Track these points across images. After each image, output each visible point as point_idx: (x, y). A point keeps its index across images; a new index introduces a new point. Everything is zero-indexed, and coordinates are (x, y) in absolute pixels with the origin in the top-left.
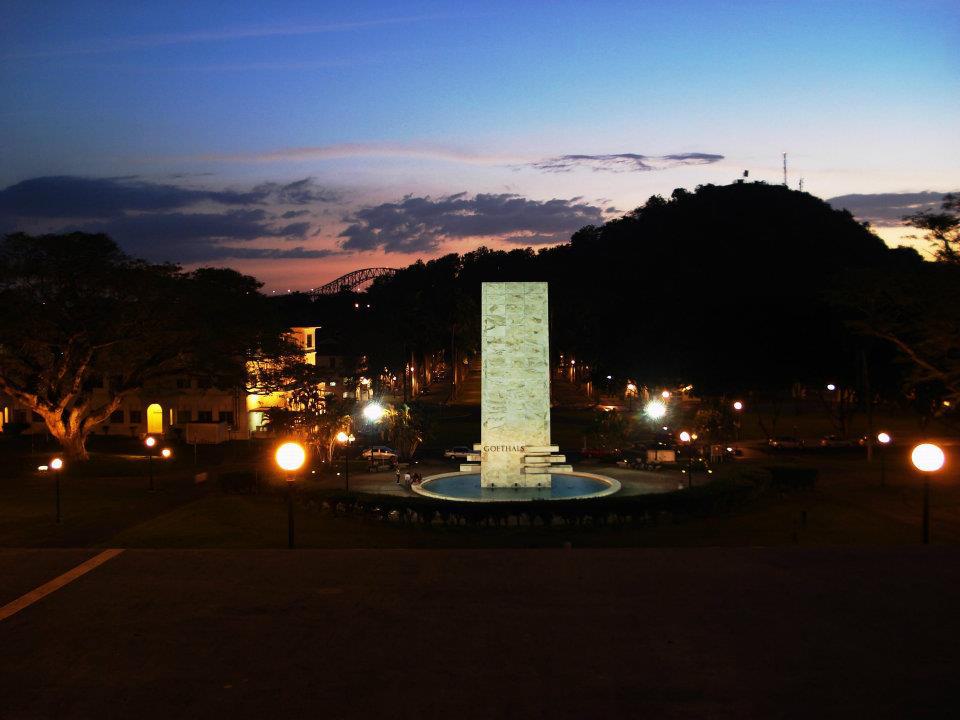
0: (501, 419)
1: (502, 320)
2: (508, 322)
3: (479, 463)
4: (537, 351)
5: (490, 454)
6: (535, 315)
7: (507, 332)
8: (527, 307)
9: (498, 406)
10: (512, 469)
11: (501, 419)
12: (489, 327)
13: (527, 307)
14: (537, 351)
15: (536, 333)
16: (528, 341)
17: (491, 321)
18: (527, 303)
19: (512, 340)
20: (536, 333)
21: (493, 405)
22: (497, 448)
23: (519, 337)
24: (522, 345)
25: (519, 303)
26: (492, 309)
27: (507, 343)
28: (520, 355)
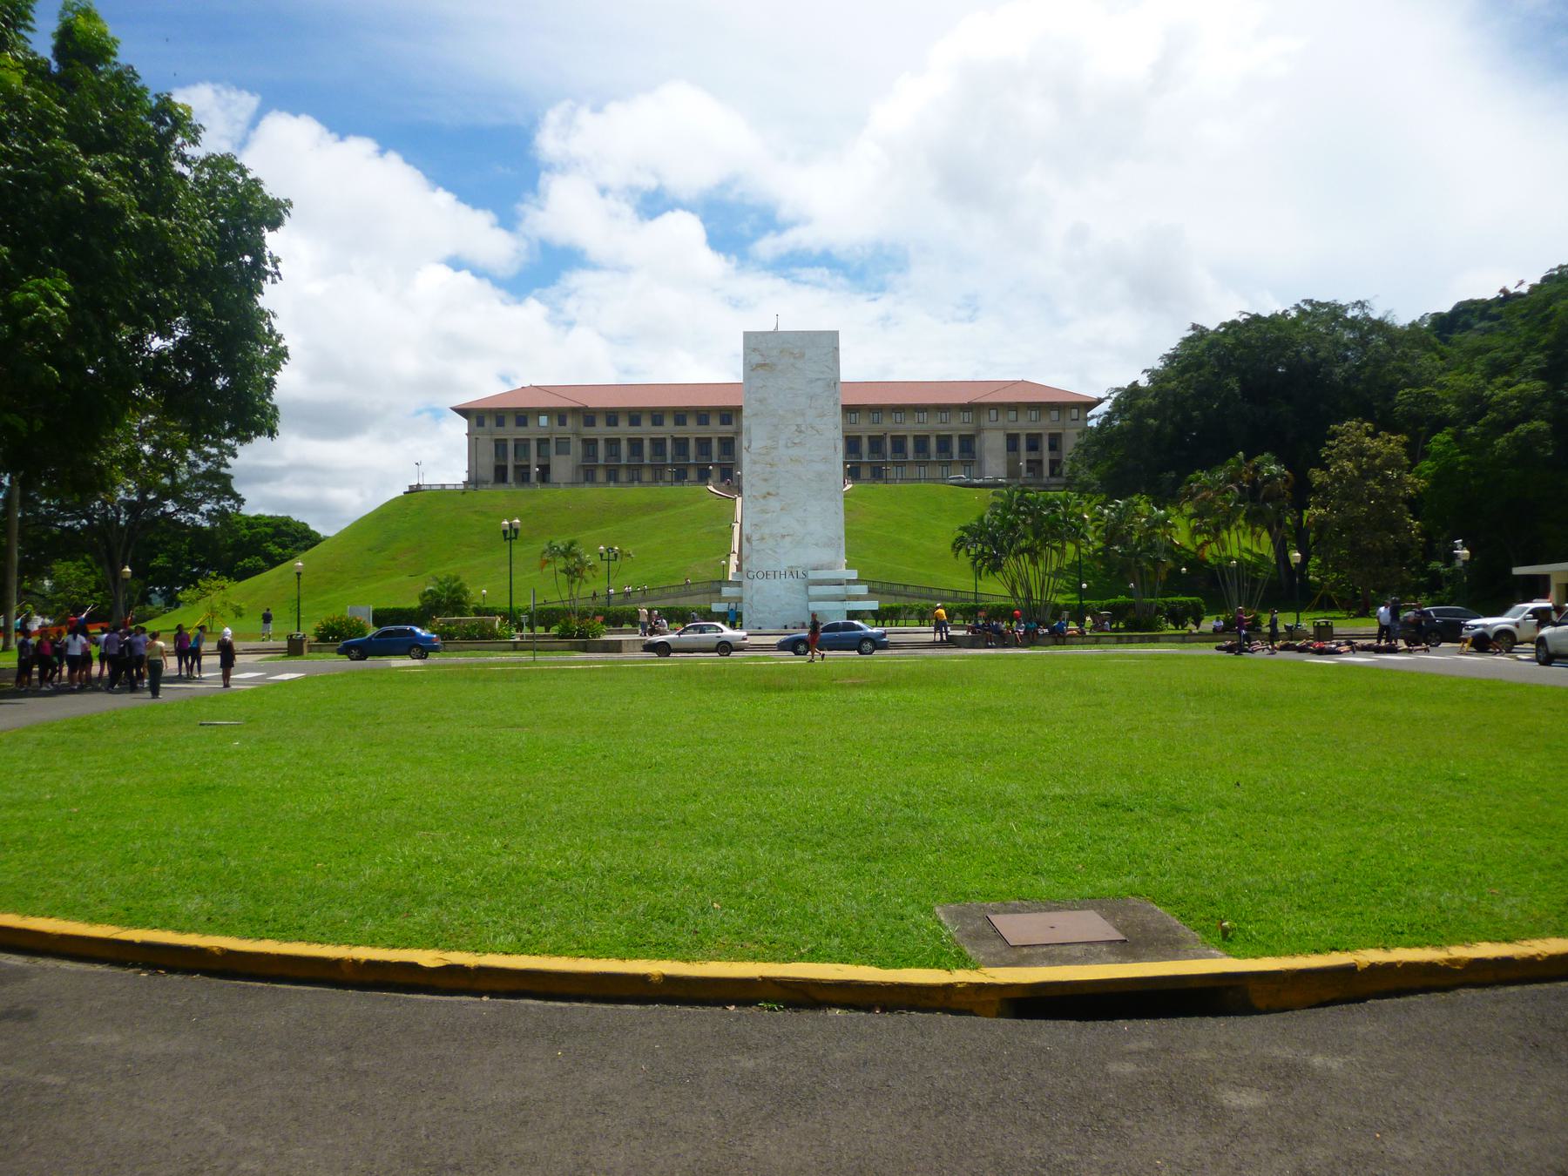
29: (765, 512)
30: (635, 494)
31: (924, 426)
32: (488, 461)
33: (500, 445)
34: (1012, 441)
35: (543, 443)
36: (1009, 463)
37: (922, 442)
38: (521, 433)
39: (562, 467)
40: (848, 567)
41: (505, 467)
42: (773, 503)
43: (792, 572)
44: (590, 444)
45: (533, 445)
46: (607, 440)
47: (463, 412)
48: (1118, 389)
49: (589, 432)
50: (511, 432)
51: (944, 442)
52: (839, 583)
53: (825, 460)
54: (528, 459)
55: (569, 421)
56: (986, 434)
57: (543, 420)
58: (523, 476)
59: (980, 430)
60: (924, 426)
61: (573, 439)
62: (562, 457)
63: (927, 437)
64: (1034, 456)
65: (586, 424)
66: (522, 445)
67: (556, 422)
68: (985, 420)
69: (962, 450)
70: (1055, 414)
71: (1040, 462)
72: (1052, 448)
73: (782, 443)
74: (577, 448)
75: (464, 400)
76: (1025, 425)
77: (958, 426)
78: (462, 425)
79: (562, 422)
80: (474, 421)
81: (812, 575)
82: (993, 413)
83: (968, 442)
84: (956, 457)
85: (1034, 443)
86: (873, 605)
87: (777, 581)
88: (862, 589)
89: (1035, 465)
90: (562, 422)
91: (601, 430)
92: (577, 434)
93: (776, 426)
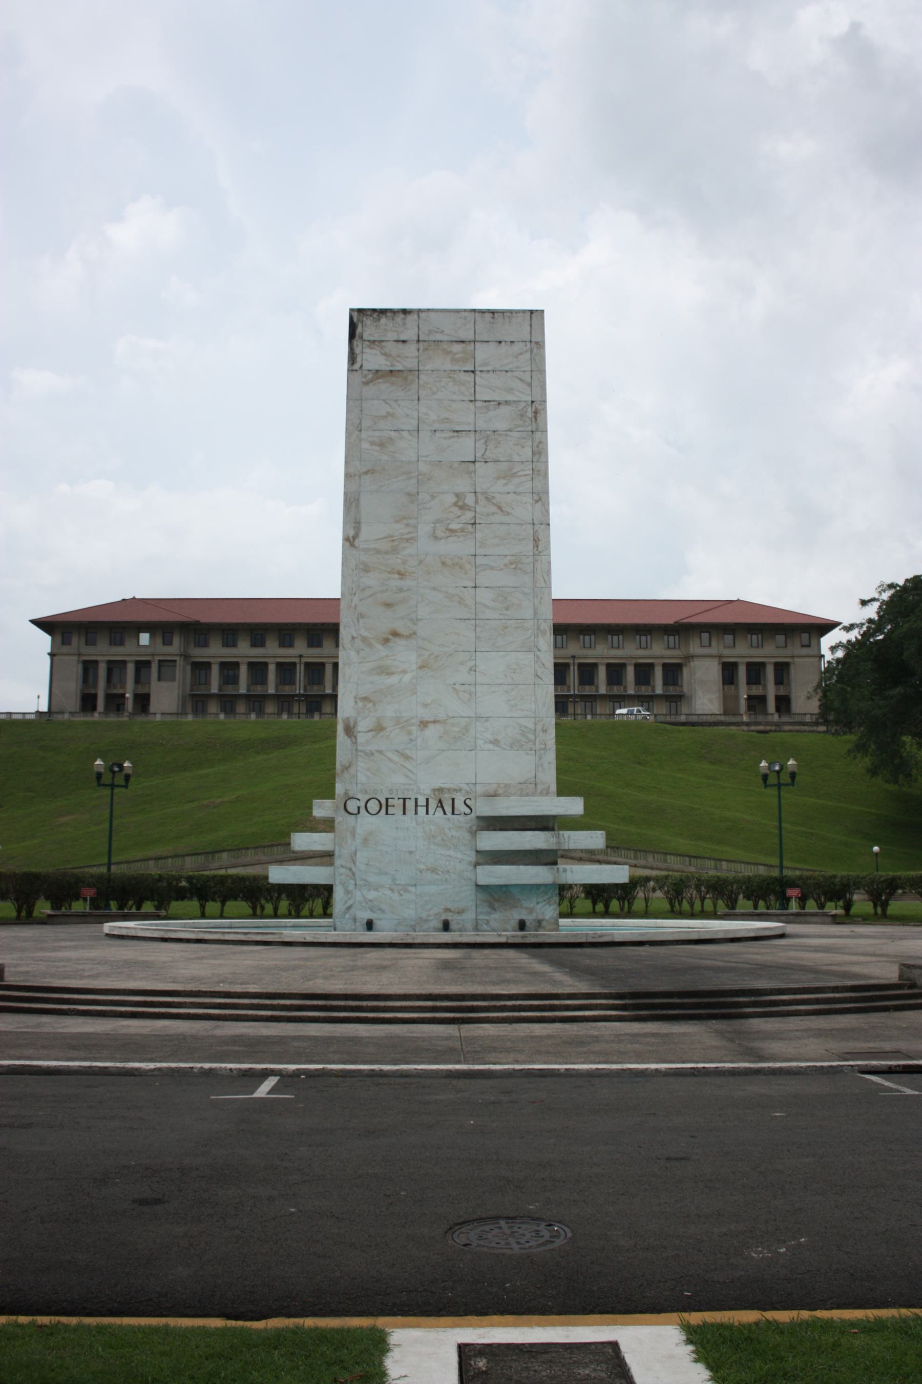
29: (386, 671)
30: (246, 725)
31: (619, 653)
32: (73, 686)
33: (89, 667)
34: (729, 671)
35: (142, 666)
36: (725, 698)
37: (615, 672)
38: (117, 653)
39: (165, 697)
40: (563, 790)
41: (94, 697)
42: (404, 656)
43: (442, 801)
44: (201, 667)
45: (131, 669)
46: (223, 665)
47: (43, 624)
48: (891, 586)
49: (200, 654)
50: (103, 651)
51: (644, 672)
52: (542, 823)
53: (515, 564)
54: (123, 686)
55: (176, 640)
56: (695, 663)
57: (145, 639)
58: (115, 702)
59: (689, 658)
60: (619, 653)
61: (180, 662)
62: (164, 684)
63: (623, 666)
64: (756, 691)
65: (198, 645)
66: (115, 667)
67: (159, 640)
68: (695, 647)
69: (666, 683)
70: (780, 638)
71: (762, 699)
72: (779, 681)
73: (424, 529)
74: (182, 671)
75: (46, 611)
76: (743, 651)
77: (659, 651)
78: (45, 640)
79: (167, 642)
80: (59, 639)
81: (485, 809)
82: (705, 636)
83: (673, 672)
84: (659, 690)
85: (755, 671)
86: (616, 874)
87: (409, 820)
88: (595, 839)
89: (756, 703)
90: (167, 642)
91: (215, 652)
92: (186, 656)
93: (412, 496)
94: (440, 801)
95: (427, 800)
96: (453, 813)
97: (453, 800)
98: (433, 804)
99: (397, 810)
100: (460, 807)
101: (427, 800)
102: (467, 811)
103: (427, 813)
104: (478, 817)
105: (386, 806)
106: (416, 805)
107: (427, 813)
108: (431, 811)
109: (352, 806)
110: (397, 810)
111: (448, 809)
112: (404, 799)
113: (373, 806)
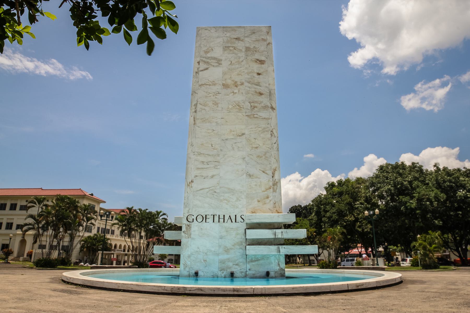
0: (212, 177)
1: (219, 62)
2: (225, 64)
3: (178, 243)
4: (261, 94)
5: (195, 226)
6: (257, 56)
7: (224, 73)
8: (248, 49)
9: (210, 159)
10: (227, 250)
11: (212, 177)
12: (200, 69)
13: (248, 49)
14: (261, 94)
15: (259, 74)
16: (249, 82)
17: (205, 62)
18: (248, 45)
19: (229, 82)
20: (259, 74)
21: (201, 158)
22: (205, 218)
23: (238, 79)
24: (241, 87)
25: (240, 45)
26: (206, 52)
27: (223, 85)
28: (239, 98)
94: (230, 216)
95: (224, 216)
96: (236, 222)
97: (236, 216)
98: (226, 218)
99: (210, 220)
100: (239, 219)
101: (224, 216)
102: (242, 221)
103: (224, 222)
104: (246, 223)
105: (205, 218)
106: (219, 218)
107: (224, 222)
108: (226, 221)
109: (190, 219)
110: (210, 220)
111: (234, 221)
112: (214, 215)
113: (200, 219)
